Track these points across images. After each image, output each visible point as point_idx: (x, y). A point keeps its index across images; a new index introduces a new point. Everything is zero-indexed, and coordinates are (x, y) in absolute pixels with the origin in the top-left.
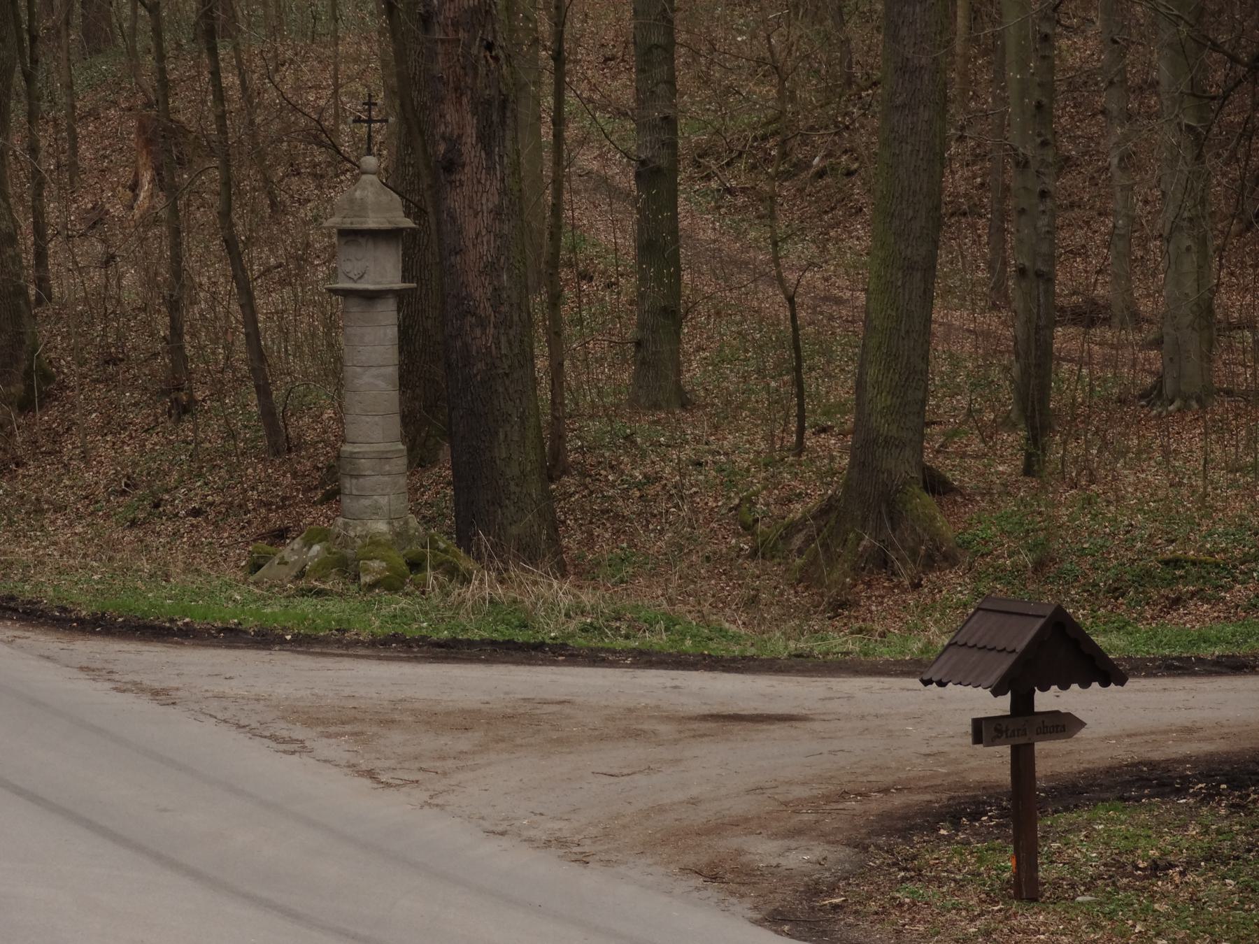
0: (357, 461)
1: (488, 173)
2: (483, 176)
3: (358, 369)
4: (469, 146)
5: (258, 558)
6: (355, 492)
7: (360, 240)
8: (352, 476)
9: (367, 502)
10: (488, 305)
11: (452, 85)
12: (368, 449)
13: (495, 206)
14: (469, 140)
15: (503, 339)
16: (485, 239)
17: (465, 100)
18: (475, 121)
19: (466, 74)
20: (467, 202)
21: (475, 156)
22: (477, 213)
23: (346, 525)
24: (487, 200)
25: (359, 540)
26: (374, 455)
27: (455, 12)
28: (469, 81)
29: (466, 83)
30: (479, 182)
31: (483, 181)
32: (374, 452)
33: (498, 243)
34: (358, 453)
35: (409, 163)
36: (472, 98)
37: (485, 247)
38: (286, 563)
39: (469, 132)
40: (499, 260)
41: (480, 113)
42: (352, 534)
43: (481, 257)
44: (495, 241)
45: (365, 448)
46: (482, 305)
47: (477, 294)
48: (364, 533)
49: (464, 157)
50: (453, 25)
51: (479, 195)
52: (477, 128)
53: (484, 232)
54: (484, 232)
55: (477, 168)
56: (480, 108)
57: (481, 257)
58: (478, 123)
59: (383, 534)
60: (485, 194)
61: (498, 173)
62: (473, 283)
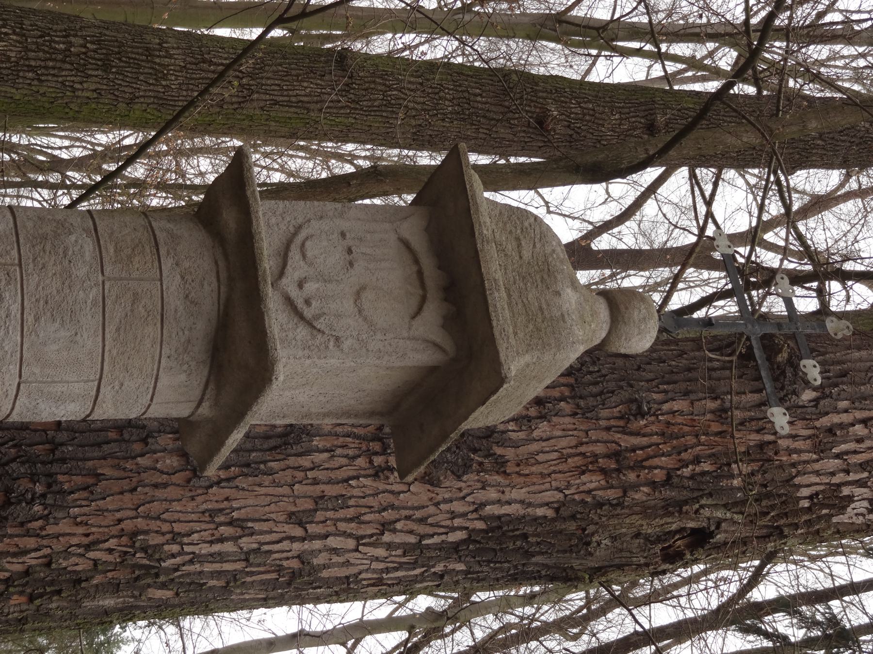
1: (407, 549)
2: (398, 538)
4: (481, 496)
7: (433, 313)
10: (31, 560)
11: (628, 441)
13: (315, 570)
14: (493, 494)
16: (228, 547)
17: (592, 481)
18: (540, 512)
19: (653, 484)
20: (331, 490)
21: (453, 515)
22: (301, 524)
24: (335, 551)
27: (790, 452)
28: (641, 495)
29: (635, 487)
30: (386, 526)
31: (387, 537)
33: (212, 583)
35: (71, 44)
36: (600, 505)
37: (205, 549)
39: (515, 494)
40: (164, 586)
41: (560, 526)
43: (175, 537)
44: (218, 574)
46: (31, 542)
47: (64, 527)
49: (450, 482)
50: (762, 446)
51: (351, 527)
52: (521, 519)
53: (247, 543)
54: (247, 543)
55: (422, 521)
56: (572, 526)
57: (175, 537)
58: (536, 519)
60: (351, 543)
61: (400, 574)
62: (101, 511)
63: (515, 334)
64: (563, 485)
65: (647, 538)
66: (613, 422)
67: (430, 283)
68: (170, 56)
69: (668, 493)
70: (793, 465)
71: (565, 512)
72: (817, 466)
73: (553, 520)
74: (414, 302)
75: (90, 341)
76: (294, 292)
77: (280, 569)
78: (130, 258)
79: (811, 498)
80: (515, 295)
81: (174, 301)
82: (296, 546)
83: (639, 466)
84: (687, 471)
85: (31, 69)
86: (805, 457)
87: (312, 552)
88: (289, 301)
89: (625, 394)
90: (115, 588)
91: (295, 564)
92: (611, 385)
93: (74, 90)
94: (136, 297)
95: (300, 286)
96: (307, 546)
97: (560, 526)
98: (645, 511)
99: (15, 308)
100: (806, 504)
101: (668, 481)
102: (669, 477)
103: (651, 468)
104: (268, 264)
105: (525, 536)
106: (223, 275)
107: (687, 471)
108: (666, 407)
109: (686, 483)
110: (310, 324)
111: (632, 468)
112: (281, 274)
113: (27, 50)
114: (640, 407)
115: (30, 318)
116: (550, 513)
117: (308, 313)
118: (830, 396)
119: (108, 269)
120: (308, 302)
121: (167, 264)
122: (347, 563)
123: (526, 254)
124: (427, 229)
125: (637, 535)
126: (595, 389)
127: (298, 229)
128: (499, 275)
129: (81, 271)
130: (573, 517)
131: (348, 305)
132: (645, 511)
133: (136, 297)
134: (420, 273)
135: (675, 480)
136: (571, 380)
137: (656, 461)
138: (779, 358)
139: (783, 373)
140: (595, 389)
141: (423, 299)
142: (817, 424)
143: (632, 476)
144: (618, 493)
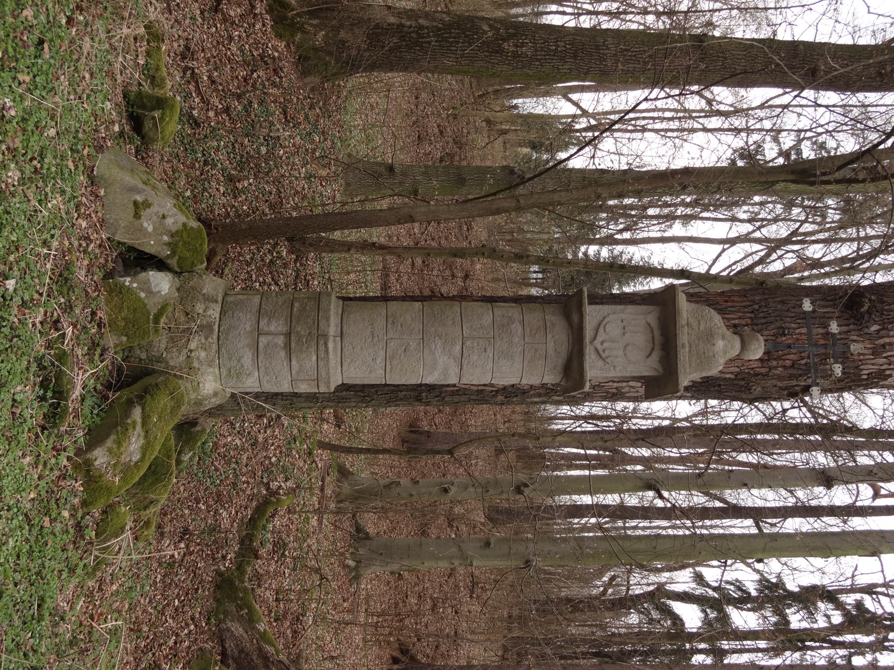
0: (313, 349)
3: (458, 348)
5: (154, 118)
6: (263, 340)
7: (656, 355)
8: (288, 335)
9: (247, 360)
12: (332, 363)
15: (463, 398)
18: (728, 376)
19: (785, 367)
23: (206, 329)
24: (632, 387)
25: (182, 358)
26: (324, 374)
29: (776, 368)
32: (328, 374)
34: (327, 351)
35: (558, 46)
36: (757, 375)
38: (137, 216)
41: (736, 382)
42: (193, 345)
45: (334, 359)
48: (196, 364)
56: (743, 383)
58: (725, 379)
59: (196, 388)
63: (690, 365)
64: (740, 365)
65: (780, 387)
66: (769, 338)
67: (657, 342)
68: (608, 49)
69: (791, 371)
70: (861, 360)
71: (739, 377)
72: (873, 362)
73: (734, 379)
74: (649, 350)
75: (518, 366)
76: (599, 347)
77: (607, 392)
78: (535, 334)
79: (868, 374)
80: (693, 347)
81: (551, 352)
82: (615, 385)
83: (778, 358)
84: (803, 362)
85: (538, 60)
86: (867, 357)
87: (622, 387)
88: (597, 350)
89: (778, 324)
90: (540, 395)
91: (614, 391)
92: (772, 319)
93: (558, 69)
94: (536, 350)
95: (602, 344)
96: (620, 384)
97: (736, 382)
98: (780, 378)
99: (491, 355)
100: (865, 377)
101: (792, 366)
102: (793, 364)
103: (784, 360)
104: (587, 339)
105: (720, 385)
106: (571, 342)
107: (803, 362)
108: (797, 331)
109: (802, 367)
110: (604, 360)
111: (775, 359)
112: (595, 338)
113: (536, 51)
114: (784, 331)
115: (496, 358)
116: (732, 376)
117: (604, 355)
118: (887, 329)
119: (526, 339)
120: (604, 351)
121: (549, 336)
122: (637, 391)
123: (702, 328)
124: (659, 318)
125: (775, 386)
126: (763, 321)
127: (604, 318)
128: (686, 342)
129: (516, 340)
130: (743, 379)
131: (621, 353)
132: (780, 378)
133: (536, 350)
134: (653, 337)
135: (796, 366)
136: (753, 315)
137: (788, 357)
138: (862, 310)
139: (863, 317)
140: (763, 321)
141: (653, 349)
142: (877, 342)
143: (774, 363)
144: (767, 370)
